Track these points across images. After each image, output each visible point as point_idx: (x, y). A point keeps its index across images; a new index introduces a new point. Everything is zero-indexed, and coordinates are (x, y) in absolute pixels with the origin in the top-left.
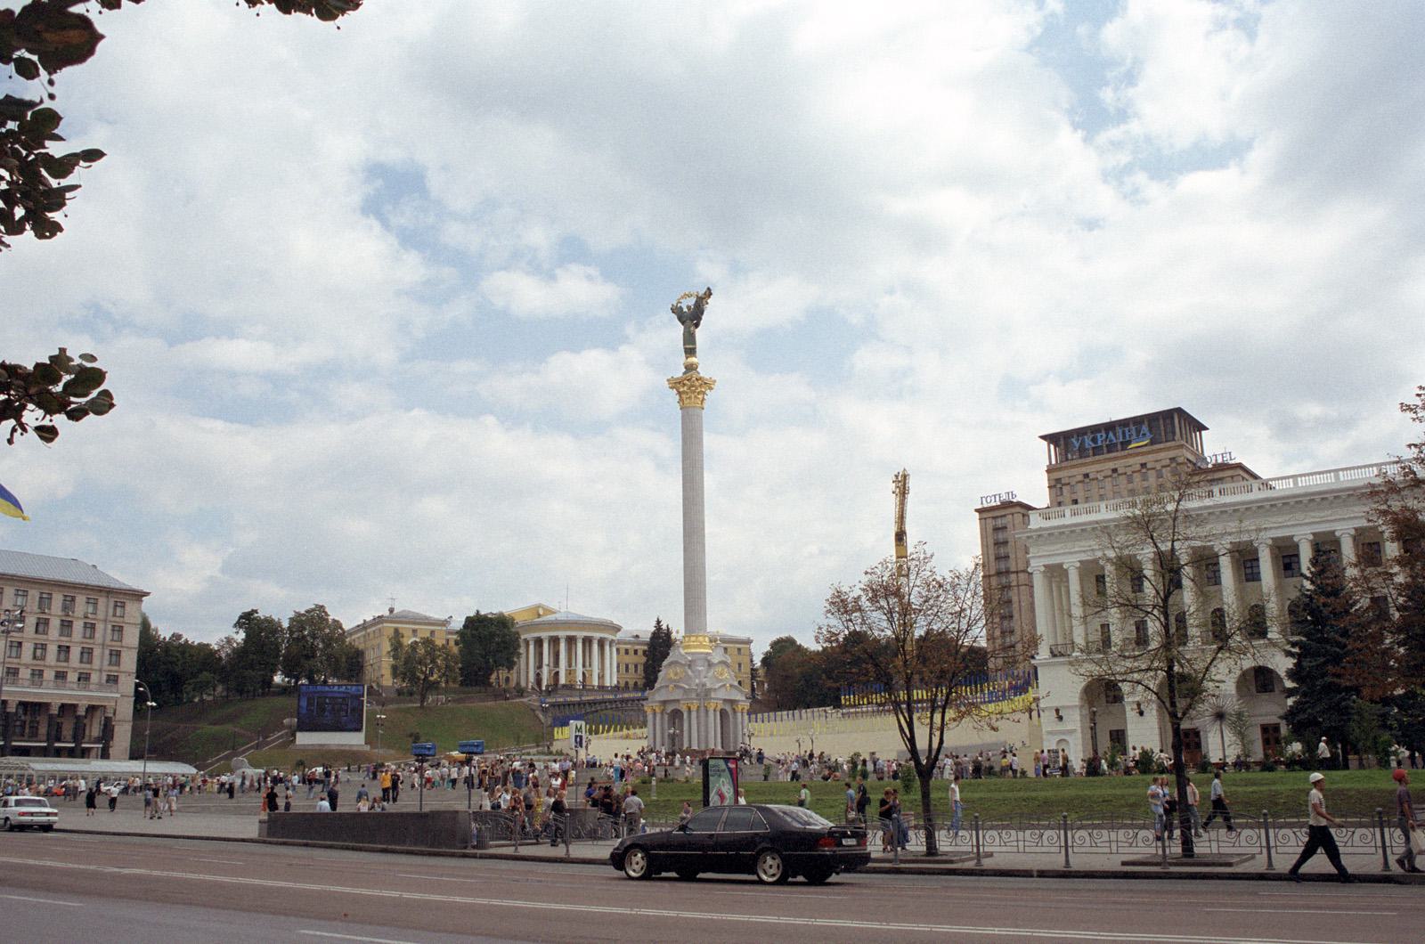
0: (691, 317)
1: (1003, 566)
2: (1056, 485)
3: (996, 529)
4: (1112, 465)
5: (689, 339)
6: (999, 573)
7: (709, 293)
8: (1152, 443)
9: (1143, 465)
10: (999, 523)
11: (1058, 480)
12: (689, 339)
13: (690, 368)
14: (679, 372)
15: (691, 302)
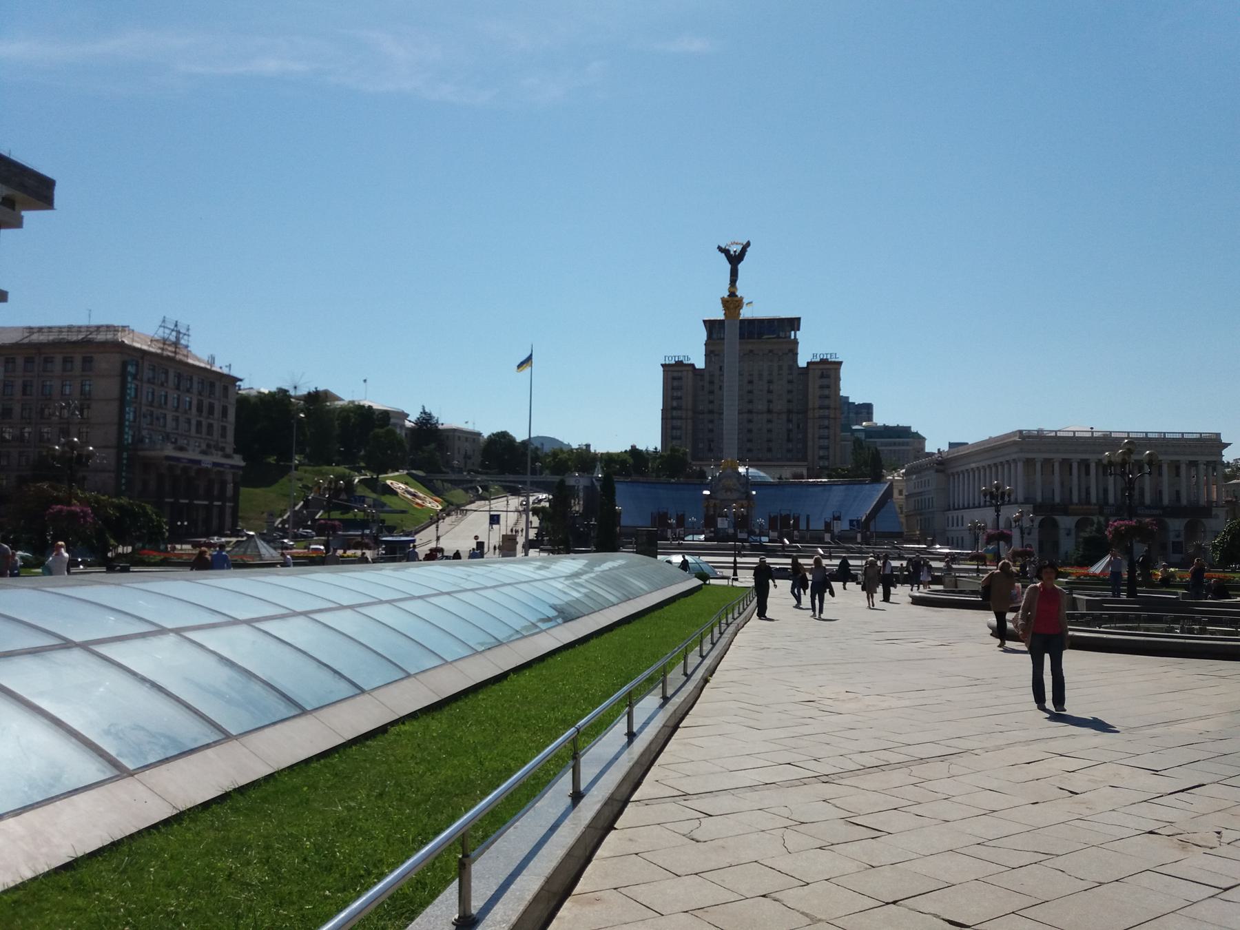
0: (735, 260)
1: (675, 404)
2: (709, 355)
3: (674, 378)
4: (750, 347)
5: (734, 275)
6: (674, 408)
7: (748, 244)
8: (779, 337)
9: (771, 351)
10: (676, 374)
11: (712, 352)
12: (734, 275)
13: (732, 294)
14: (726, 294)
15: (739, 248)
